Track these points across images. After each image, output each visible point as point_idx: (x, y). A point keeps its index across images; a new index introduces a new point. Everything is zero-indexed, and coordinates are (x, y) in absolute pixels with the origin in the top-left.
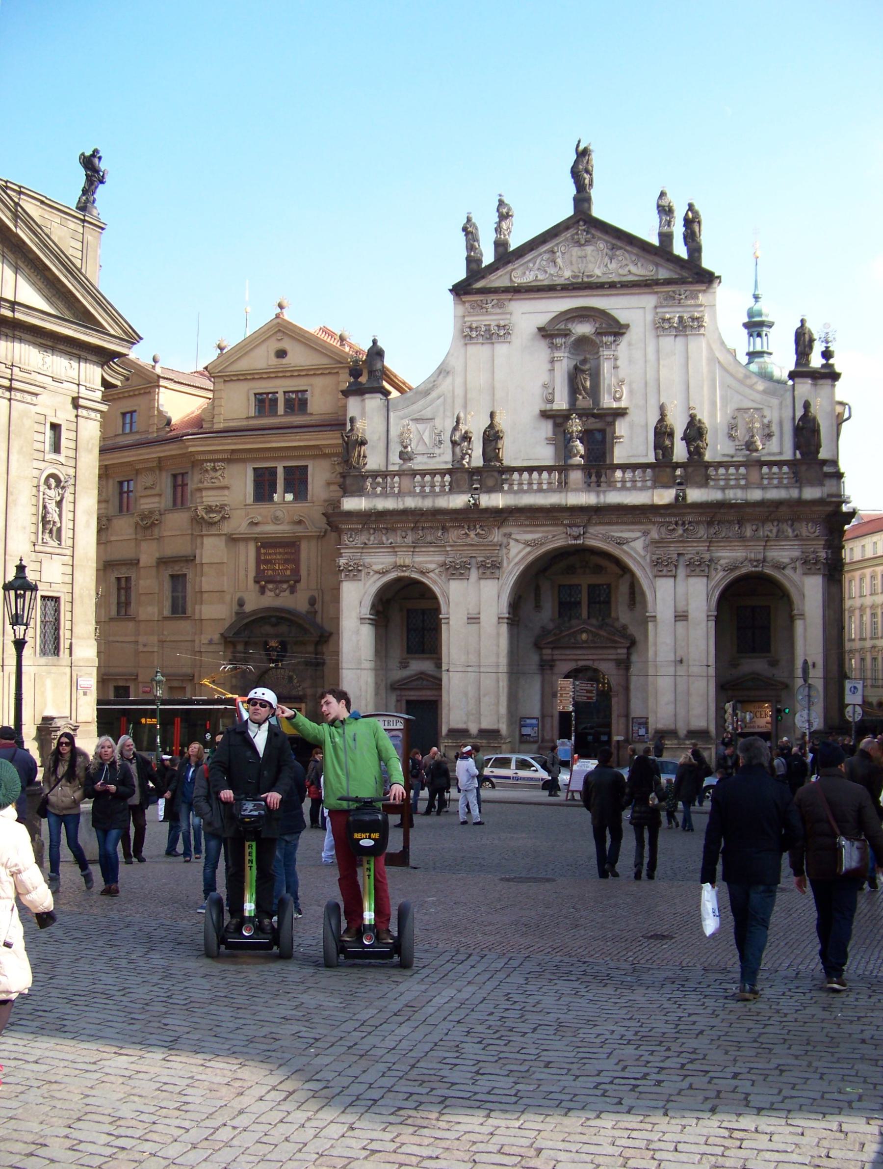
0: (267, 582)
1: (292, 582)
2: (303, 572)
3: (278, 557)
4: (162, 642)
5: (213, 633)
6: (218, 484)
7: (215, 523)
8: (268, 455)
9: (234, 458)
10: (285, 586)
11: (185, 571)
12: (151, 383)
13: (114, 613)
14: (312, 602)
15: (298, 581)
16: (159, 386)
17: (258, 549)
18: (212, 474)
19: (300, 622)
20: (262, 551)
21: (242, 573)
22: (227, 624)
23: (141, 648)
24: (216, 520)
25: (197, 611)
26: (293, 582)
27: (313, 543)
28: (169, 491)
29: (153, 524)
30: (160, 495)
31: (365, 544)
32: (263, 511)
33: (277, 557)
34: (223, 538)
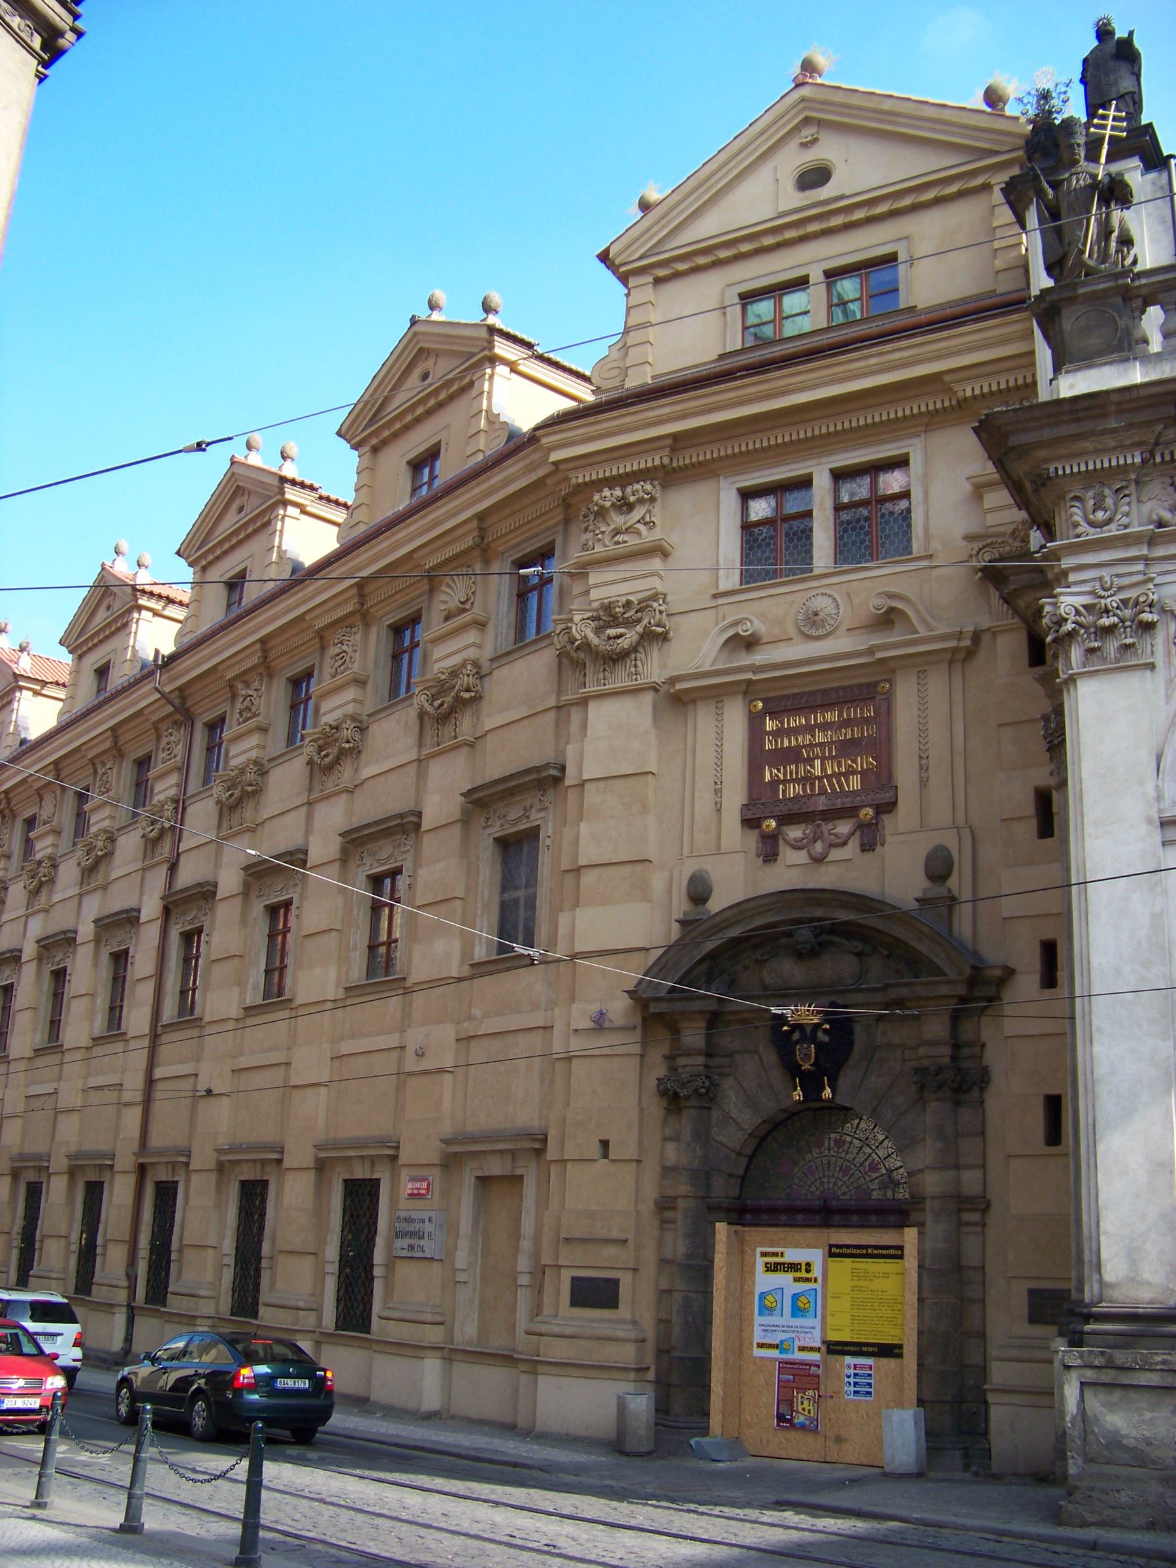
0: (785, 820)
2: (905, 775)
3: (820, 737)
4: (466, 1040)
5: (609, 991)
6: (632, 541)
8: (781, 437)
9: (681, 465)
10: (843, 828)
11: (535, 817)
12: (473, 355)
14: (939, 867)
15: (887, 807)
16: (494, 360)
17: (755, 722)
18: (618, 520)
19: (897, 931)
20: (769, 725)
23: (411, 1064)
24: (624, 643)
25: (563, 930)
27: (936, 683)
29: (460, 704)
30: (481, 625)
31: (1161, 524)
32: (771, 609)
33: (818, 720)
34: (648, 698)
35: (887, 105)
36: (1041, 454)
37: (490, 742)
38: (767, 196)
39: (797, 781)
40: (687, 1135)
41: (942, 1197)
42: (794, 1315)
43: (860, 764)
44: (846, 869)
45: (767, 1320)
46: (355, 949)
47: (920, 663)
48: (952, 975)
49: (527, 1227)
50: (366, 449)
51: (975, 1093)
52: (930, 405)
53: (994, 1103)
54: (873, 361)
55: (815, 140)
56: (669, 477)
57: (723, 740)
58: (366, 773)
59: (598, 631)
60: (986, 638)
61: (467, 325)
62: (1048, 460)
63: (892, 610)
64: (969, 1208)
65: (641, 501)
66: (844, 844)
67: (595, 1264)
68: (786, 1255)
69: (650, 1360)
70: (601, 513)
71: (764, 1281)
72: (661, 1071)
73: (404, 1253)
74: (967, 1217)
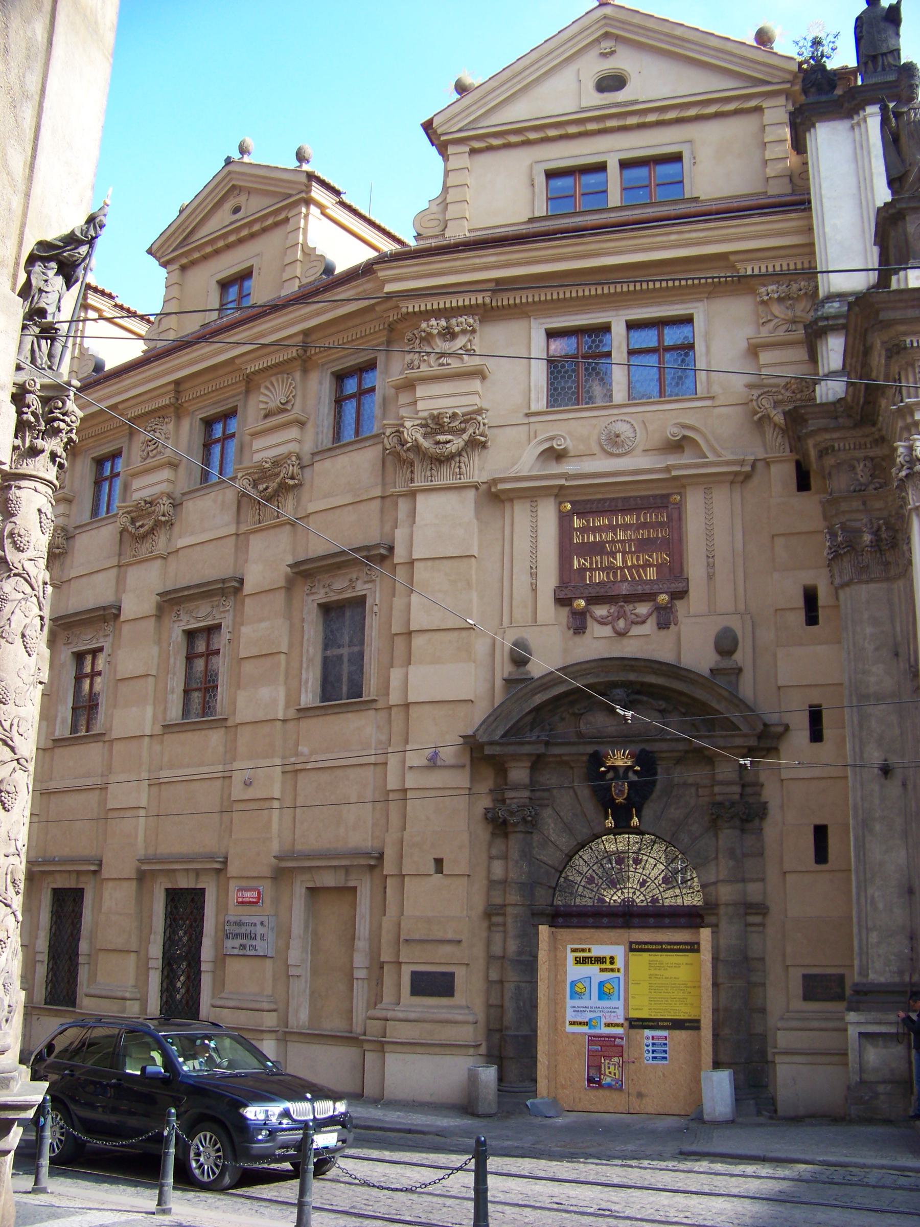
0: (594, 600)
1: (663, 598)
2: (695, 570)
3: (621, 536)
5: (441, 734)
6: (455, 364)
7: (450, 457)
9: (500, 303)
10: (643, 609)
11: (361, 588)
12: (290, 196)
13: (174, 712)
14: (726, 645)
15: (680, 594)
16: (308, 202)
17: (564, 520)
18: (441, 346)
19: (700, 694)
20: (577, 523)
21: (522, 581)
22: (479, 714)
23: (238, 792)
24: (452, 448)
26: (667, 597)
28: (326, 410)
29: (284, 489)
30: (302, 424)
32: (576, 428)
34: (471, 494)
35: (678, 32)
36: (902, 328)
37: (313, 524)
38: (569, 93)
39: (602, 569)
40: (515, 854)
41: (735, 904)
42: (600, 998)
43: (655, 558)
44: (645, 641)
45: (577, 1003)
46: (173, 692)
47: (708, 481)
48: (745, 729)
49: (363, 928)
50: (176, 266)
51: (757, 822)
52: (724, 278)
53: (771, 830)
54: (673, 237)
55: (612, 53)
56: (488, 314)
57: (538, 533)
58: (181, 543)
59: (425, 436)
60: (759, 465)
61: (285, 170)
62: (905, 334)
63: (684, 437)
64: (753, 910)
65: (464, 332)
66: (643, 622)
67: (432, 961)
68: (592, 950)
69: (481, 1038)
70: (428, 338)
71: (574, 972)
72: (486, 802)
73: (236, 952)
74: (752, 919)
